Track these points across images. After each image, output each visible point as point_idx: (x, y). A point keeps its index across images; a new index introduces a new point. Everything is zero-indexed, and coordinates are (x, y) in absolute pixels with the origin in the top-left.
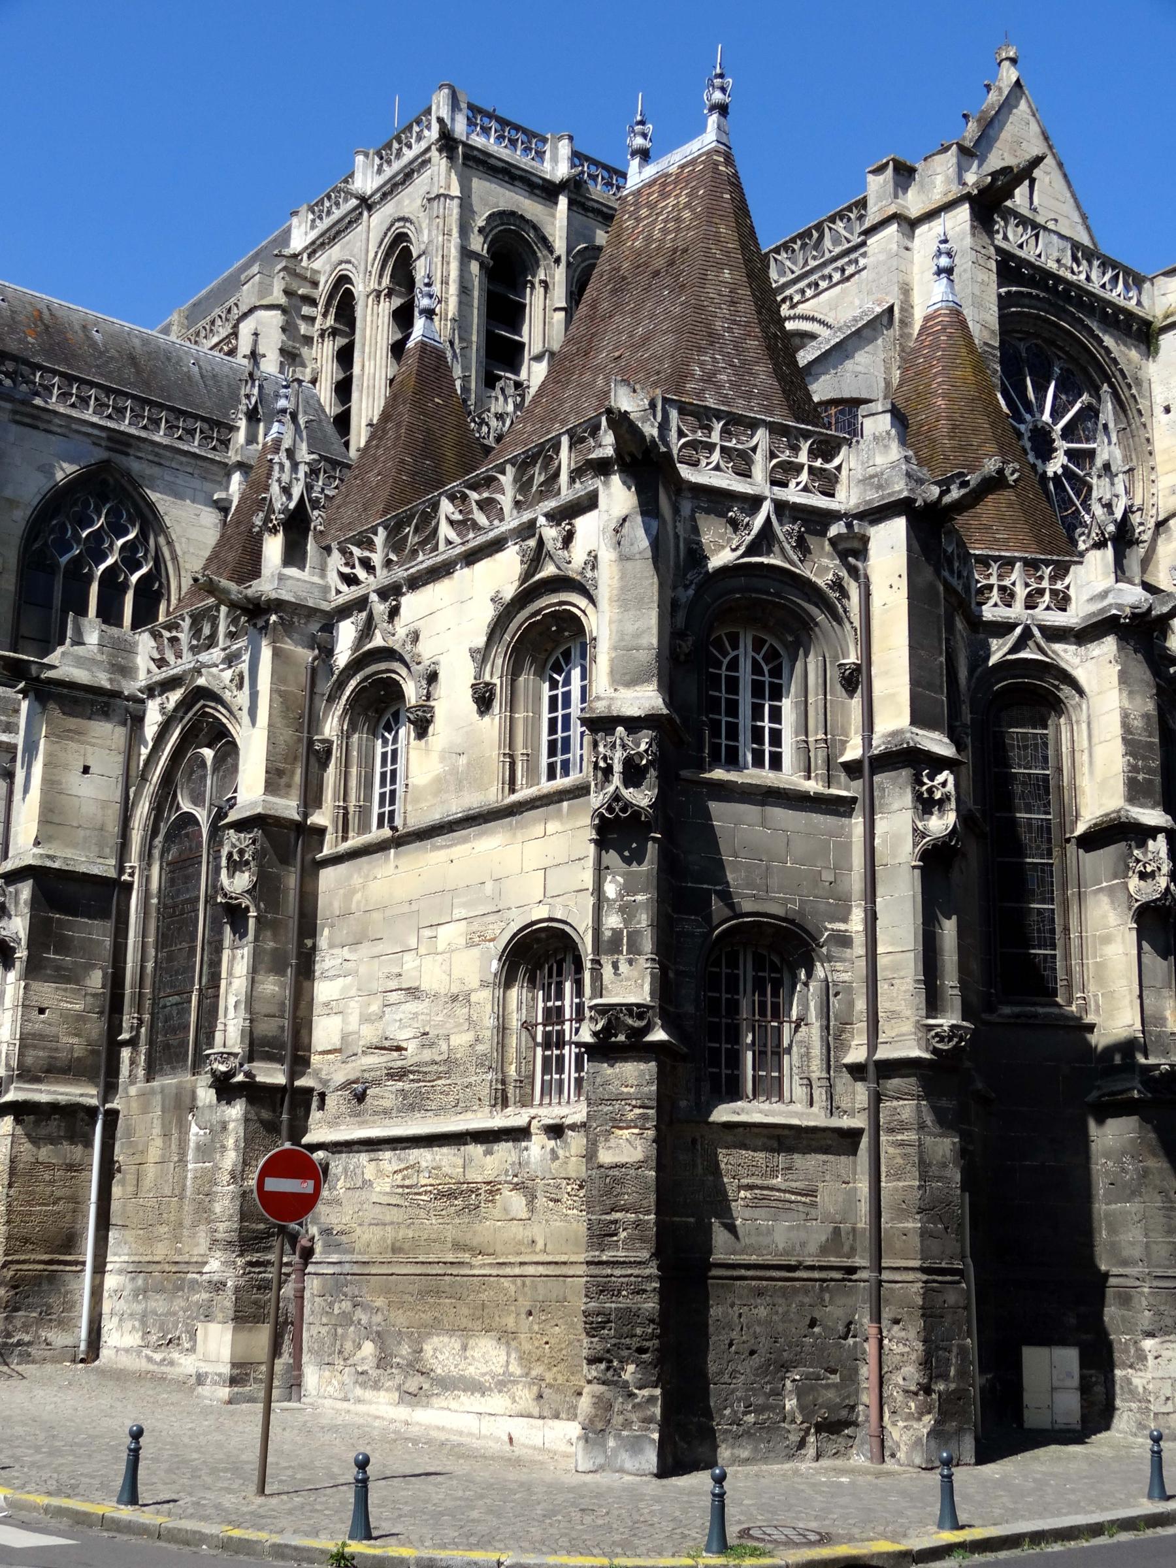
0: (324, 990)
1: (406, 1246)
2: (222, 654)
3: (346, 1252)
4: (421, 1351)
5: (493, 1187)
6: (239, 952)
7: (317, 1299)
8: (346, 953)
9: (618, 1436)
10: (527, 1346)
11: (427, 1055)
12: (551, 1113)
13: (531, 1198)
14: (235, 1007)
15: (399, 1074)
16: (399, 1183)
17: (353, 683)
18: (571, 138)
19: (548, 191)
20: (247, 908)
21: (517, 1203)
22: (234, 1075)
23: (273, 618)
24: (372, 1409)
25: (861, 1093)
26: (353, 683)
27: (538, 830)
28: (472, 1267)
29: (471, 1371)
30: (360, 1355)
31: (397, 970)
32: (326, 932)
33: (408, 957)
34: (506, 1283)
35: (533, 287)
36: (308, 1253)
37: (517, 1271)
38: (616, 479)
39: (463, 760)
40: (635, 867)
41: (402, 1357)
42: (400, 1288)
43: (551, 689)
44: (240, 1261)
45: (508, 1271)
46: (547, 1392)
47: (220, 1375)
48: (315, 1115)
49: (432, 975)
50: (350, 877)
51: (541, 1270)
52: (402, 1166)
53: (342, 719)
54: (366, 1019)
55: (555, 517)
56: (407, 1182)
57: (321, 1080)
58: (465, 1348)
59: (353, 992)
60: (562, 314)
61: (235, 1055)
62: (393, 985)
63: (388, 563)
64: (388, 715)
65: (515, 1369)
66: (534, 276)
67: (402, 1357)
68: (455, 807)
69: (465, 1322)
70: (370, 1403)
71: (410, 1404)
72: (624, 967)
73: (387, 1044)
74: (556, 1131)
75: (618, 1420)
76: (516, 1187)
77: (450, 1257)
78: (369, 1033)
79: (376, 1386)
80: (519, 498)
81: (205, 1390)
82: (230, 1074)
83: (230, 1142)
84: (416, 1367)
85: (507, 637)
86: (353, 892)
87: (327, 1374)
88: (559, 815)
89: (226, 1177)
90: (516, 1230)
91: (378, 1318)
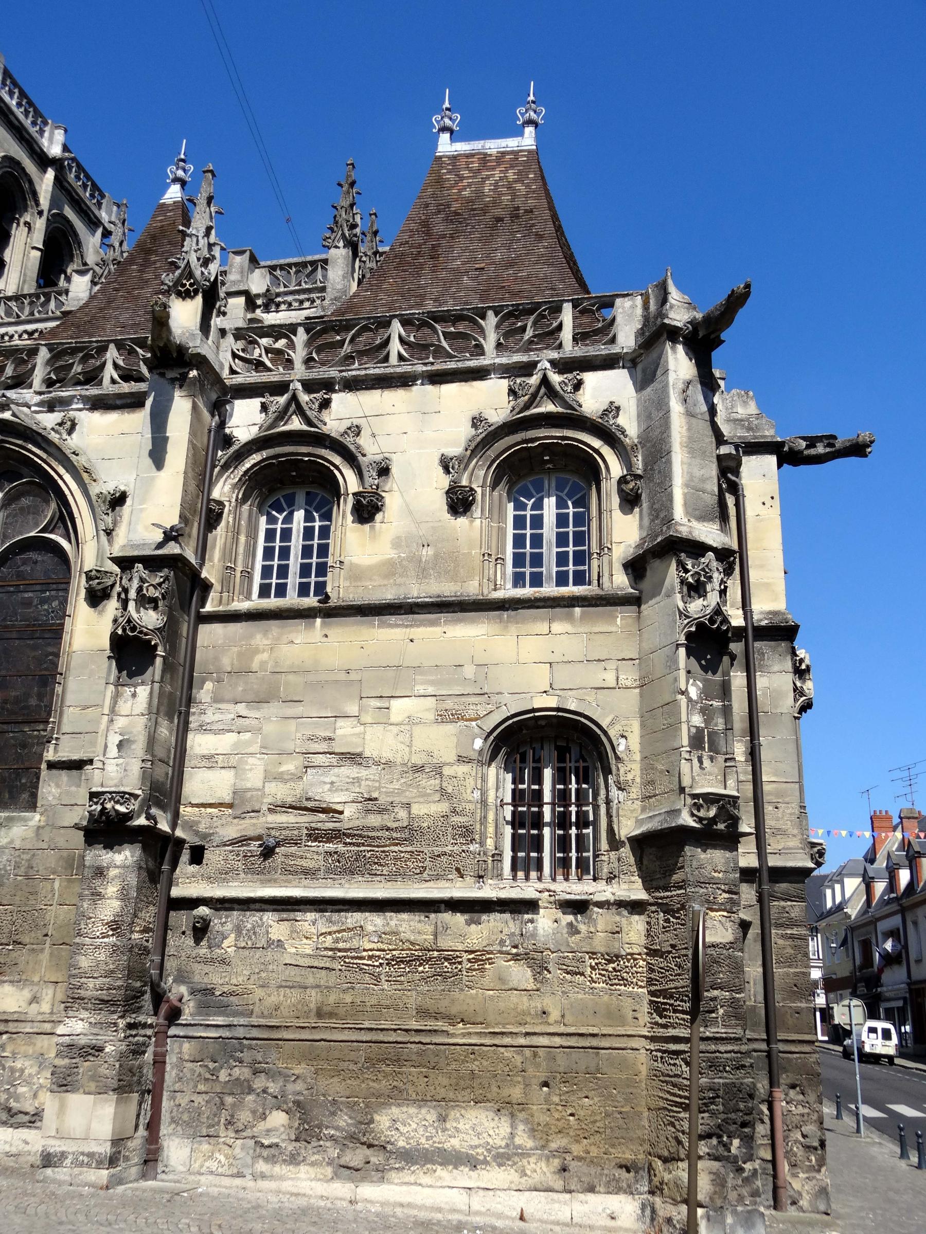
0: (199, 743)
1: (341, 1011)
2: (38, 398)
3: (236, 1014)
4: (372, 1121)
5: (481, 958)
6: (128, 691)
7: (189, 1065)
8: (241, 709)
9: (735, 1213)
10: (543, 1118)
11: (374, 820)
12: (577, 889)
13: (540, 968)
14: (120, 745)
15: (335, 835)
16: (327, 945)
17: (255, 458)
18: (66, 131)
19: (43, 161)
20: (156, 646)
21: (521, 974)
22: (131, 818)
23: (193, 373)
24: (287, 1186)
25: (748, 893)
26: (255, 458)
27: (543, 627)
28: (453, 1035)
29: (454, 1143)
30: (262, 1126)
31: (328, 734)
32: (209, 685)
33: (340, 723)
34: (508, 1053)
35: (18, 224)
36: (174, 1015)
37: (522, 1041)
38: (680, 348)
39: (430, 551)
40: (710, 676)
41: (337, 1128)
42: (336, 1054)
43: (268, 522)
44: (122, 1023)
45: (507, 1040)
46: (573, 1165)
47: (90, 1155)
48: (185, 868)
49: (379, 743)
50: (252, 636)
51: (558, 1041)
52: (335, 928)
53: (234, 486)
54: (270, 776)
55: (562, 366)
56: (341, 945)
57: (197, 833)
58: (443, 1119)
59: (255, 748)
60: (38, 254)
61: (136, 796)
62: (323, 747)
63: (308, 361)
64: (279, 496)
65: (523, 1139)
66: (21, 216)
67: (337, 1128)
68: (389, 595)
69: (442, 1093)
70: (281, 1178)
71: (351, 1180)
72: (706, 763)
73: (310, 804)
74: (578, 907)
75: (732, 1196)
76: (516, 958)
77: (414, 1025)
78: (280, 792)
79: (294, 1160)
80: (502, 340)
81: (61, 1174)
82: (128, 817)
83: (112, 890)
84: (362, 1137)
85: (491, 453)
86: (257, 651)
87: (205, 1147)
88: (570, 618)
89: (100, 929)
90: (524, 1002)
91: (299, 1086)
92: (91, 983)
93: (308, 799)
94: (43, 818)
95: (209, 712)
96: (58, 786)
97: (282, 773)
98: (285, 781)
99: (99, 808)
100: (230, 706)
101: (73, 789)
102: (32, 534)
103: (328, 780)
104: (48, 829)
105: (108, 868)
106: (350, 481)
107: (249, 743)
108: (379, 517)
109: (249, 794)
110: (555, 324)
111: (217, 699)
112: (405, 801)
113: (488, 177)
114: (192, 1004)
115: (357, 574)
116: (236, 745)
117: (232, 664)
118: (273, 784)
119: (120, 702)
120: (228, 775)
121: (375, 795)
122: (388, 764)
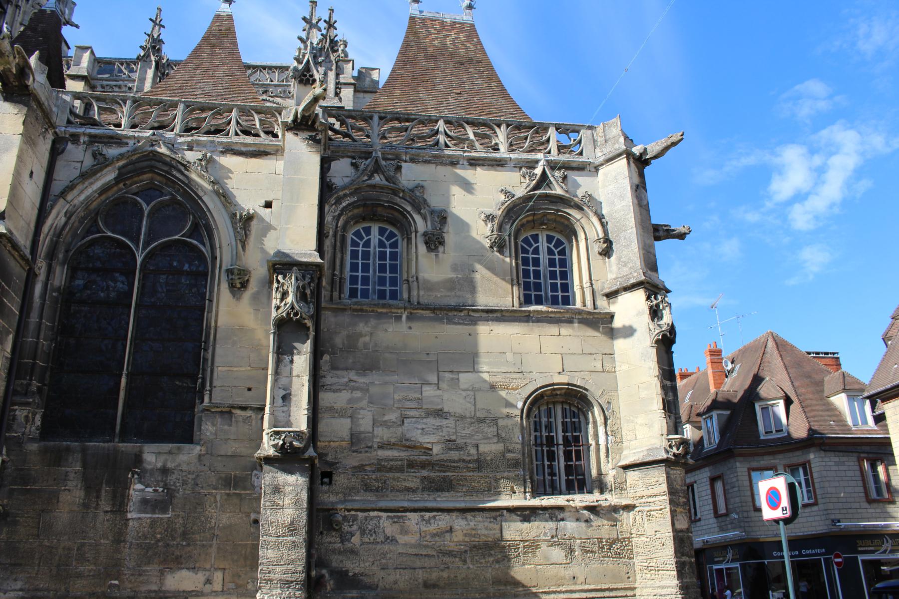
1: (442, 584)
8: (352, 375)
11: (455, 455)
33: (425, 388)
59: (364, 403)
73: (408, 444)
78: (383, 434)
86: (361, 335)
92: (278, 569)
93: (407, 440)
94: (203, 449)
95: (329, 378)
96: (213, 425)
97: (386, 421)
98: (389, 427)
99: (281, 442)
100: (344, 373)
101: (226, 427)
102: (176, 237)
103: (420, 427)
104: (207, 456)
105: (284, 486)
106: (421, 225)
107: (359, 400)
108: (441, 249)
109: (363, 436)
110: (544, 138)
111: (334, 367)
112: (474, 442)
113: (448, 36)
114: (332, 582)
115: (430, 287)
116: (350, 401)
117: (343, 343)
118: (380, 429)
119: (282, 367)
120: (347, 422)
121: (454, 438)
122: (462, 418)
